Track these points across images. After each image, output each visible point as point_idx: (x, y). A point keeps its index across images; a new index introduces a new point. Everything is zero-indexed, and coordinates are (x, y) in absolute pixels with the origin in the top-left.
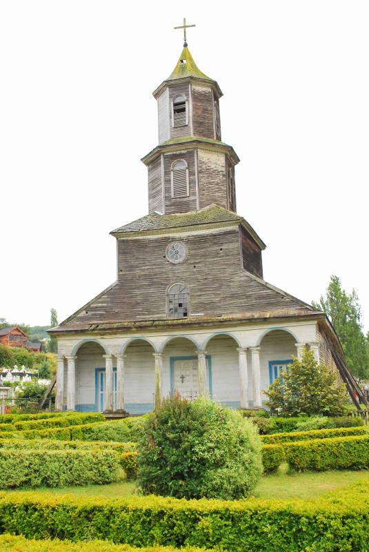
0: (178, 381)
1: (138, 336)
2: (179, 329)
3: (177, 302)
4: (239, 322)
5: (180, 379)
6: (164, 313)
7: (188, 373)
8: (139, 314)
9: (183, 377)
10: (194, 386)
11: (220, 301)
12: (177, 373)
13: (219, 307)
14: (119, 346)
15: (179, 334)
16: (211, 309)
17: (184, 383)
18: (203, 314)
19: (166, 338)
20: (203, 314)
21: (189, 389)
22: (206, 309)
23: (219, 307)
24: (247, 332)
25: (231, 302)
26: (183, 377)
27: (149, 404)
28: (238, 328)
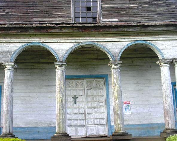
0: (70, 102)
1: (35, 41)
2: (89, 35)
3: (86, 5)
4: (166, 29)
5: (73, 100)
6: (69, 17)
7: (81, 93)
8: (37, 17)
9: (75, 98)
10: (88, 108)
11: (137, 7)
12: (69, 93)
13: (135, 14)
14: (9, 52)
15: (87, 40)
16: (127, 14)
17: (78, 103)
18: (117, 20)
19: (71, 45)
20: (117, 20)
21: (82, 111)
22: (121, 15)
23: (135, 14)
24: (170, 43)
25: (152, 9)
26: (75, 98)
27: (35, 127)
28: (160, 37)
